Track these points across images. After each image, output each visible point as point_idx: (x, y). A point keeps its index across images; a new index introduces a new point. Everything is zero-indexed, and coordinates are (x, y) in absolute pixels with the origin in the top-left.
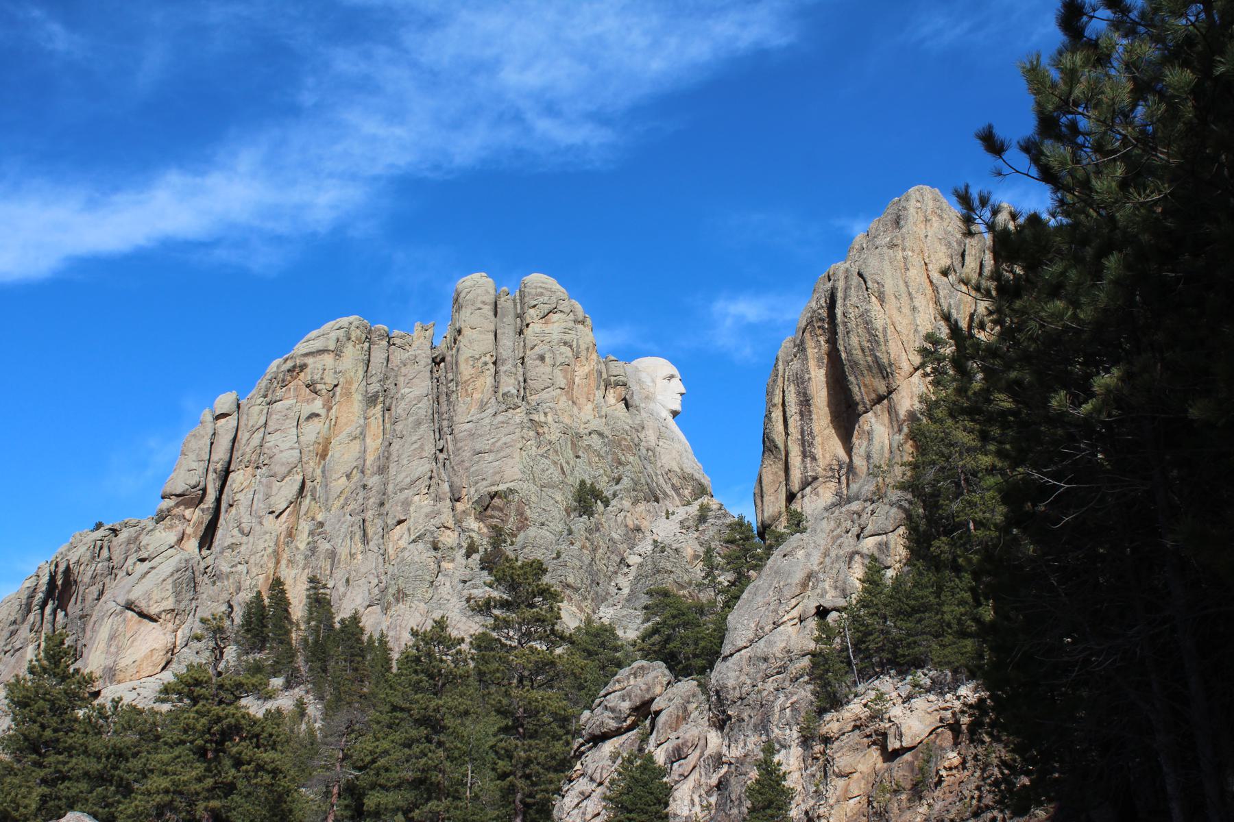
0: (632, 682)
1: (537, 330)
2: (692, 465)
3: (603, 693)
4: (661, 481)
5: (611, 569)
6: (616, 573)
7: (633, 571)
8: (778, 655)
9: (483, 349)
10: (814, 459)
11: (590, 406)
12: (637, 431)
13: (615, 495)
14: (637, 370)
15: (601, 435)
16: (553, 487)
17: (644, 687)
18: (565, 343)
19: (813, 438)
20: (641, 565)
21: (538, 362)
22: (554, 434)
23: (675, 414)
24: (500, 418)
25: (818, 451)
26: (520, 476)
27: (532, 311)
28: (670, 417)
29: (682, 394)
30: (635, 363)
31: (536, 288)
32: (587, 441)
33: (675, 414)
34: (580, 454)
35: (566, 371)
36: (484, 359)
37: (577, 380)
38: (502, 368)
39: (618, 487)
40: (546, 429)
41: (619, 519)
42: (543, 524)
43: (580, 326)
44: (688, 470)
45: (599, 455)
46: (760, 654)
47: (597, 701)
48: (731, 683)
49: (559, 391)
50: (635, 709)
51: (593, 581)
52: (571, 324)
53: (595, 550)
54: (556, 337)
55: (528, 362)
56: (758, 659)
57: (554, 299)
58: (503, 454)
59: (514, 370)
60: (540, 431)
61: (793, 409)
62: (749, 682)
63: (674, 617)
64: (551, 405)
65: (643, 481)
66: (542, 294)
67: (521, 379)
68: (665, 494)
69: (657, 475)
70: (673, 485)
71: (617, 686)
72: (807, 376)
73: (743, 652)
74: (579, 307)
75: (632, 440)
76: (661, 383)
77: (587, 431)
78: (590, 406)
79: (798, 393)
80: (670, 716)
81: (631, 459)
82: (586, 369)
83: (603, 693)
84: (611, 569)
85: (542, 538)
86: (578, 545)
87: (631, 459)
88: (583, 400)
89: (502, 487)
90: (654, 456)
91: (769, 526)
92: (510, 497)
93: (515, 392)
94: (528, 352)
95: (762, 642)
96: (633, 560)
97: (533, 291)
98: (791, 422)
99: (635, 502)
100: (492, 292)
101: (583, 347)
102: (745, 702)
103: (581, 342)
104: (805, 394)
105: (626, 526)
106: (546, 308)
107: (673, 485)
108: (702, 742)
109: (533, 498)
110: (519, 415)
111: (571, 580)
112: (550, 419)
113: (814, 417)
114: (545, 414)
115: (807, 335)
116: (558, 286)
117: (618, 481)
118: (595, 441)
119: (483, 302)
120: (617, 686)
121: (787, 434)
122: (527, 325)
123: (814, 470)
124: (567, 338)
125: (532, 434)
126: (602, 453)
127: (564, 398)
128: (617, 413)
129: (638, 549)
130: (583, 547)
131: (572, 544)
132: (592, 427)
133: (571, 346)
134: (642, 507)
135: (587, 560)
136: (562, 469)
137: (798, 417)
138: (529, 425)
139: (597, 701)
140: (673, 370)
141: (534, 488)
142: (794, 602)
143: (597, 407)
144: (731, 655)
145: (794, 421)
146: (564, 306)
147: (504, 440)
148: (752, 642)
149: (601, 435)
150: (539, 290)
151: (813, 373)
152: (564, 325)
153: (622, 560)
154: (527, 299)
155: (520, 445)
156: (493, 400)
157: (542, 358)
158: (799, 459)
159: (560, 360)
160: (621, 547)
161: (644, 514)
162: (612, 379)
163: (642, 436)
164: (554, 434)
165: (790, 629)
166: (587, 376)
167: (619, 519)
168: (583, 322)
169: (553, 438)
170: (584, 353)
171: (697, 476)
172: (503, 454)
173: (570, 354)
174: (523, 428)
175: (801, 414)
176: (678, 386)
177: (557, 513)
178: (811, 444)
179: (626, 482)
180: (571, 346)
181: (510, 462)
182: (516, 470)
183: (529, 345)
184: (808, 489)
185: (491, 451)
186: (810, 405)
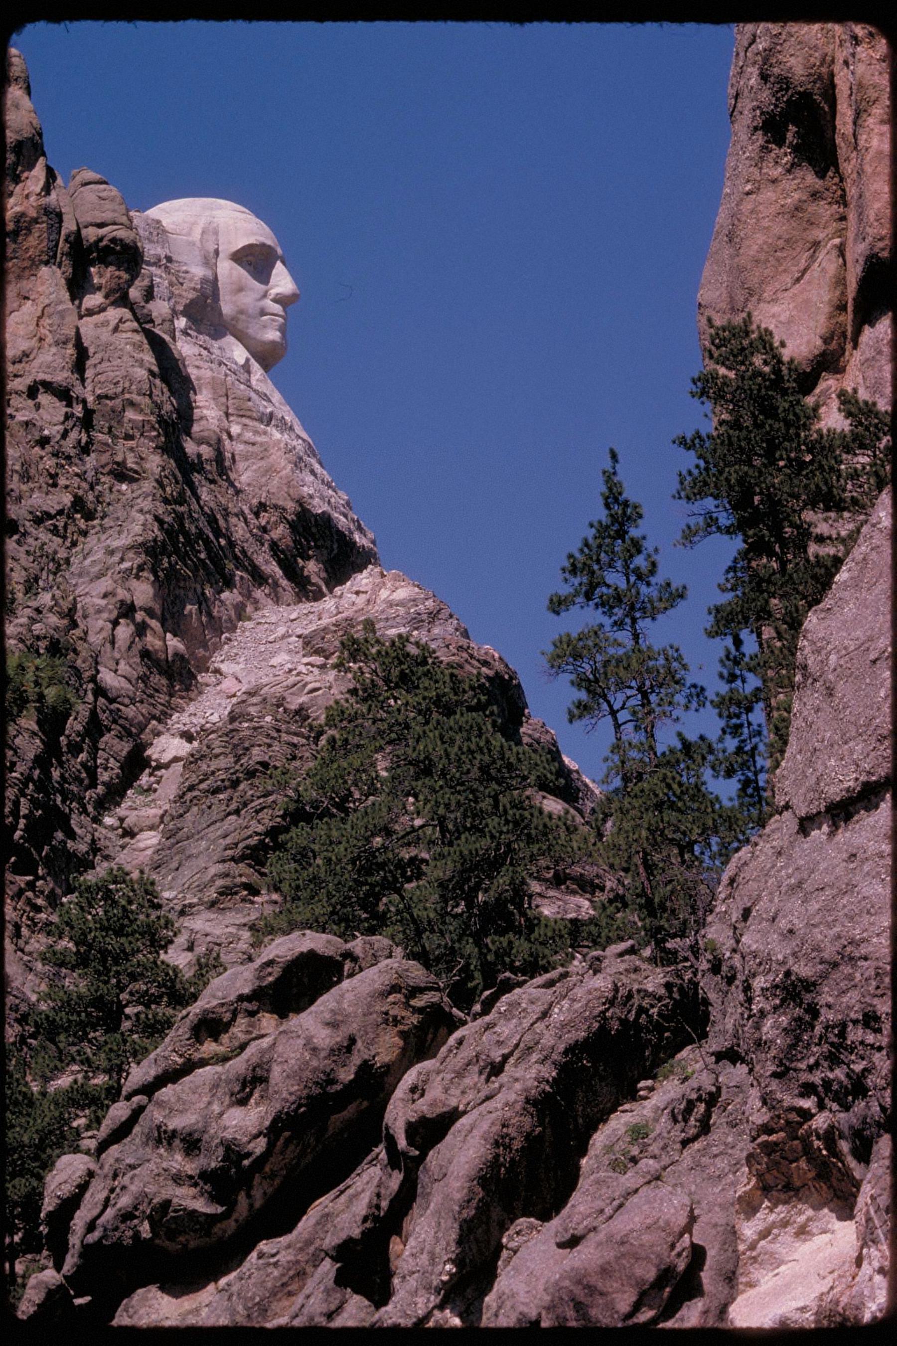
2: (322, 495)
3: (139, 1073)
4: (239, 531)
7: (170, 784)
15: (64, 394)
20: (193, 760)
33: (267, 356)
44: (318, 507)
45: (56, 455)
69: (226, 514)
80: (500, 1142)
83: (139, 1073)
91: (618, 594)
105: (145, 654)
132: (35, 372)
160: (130, 712)
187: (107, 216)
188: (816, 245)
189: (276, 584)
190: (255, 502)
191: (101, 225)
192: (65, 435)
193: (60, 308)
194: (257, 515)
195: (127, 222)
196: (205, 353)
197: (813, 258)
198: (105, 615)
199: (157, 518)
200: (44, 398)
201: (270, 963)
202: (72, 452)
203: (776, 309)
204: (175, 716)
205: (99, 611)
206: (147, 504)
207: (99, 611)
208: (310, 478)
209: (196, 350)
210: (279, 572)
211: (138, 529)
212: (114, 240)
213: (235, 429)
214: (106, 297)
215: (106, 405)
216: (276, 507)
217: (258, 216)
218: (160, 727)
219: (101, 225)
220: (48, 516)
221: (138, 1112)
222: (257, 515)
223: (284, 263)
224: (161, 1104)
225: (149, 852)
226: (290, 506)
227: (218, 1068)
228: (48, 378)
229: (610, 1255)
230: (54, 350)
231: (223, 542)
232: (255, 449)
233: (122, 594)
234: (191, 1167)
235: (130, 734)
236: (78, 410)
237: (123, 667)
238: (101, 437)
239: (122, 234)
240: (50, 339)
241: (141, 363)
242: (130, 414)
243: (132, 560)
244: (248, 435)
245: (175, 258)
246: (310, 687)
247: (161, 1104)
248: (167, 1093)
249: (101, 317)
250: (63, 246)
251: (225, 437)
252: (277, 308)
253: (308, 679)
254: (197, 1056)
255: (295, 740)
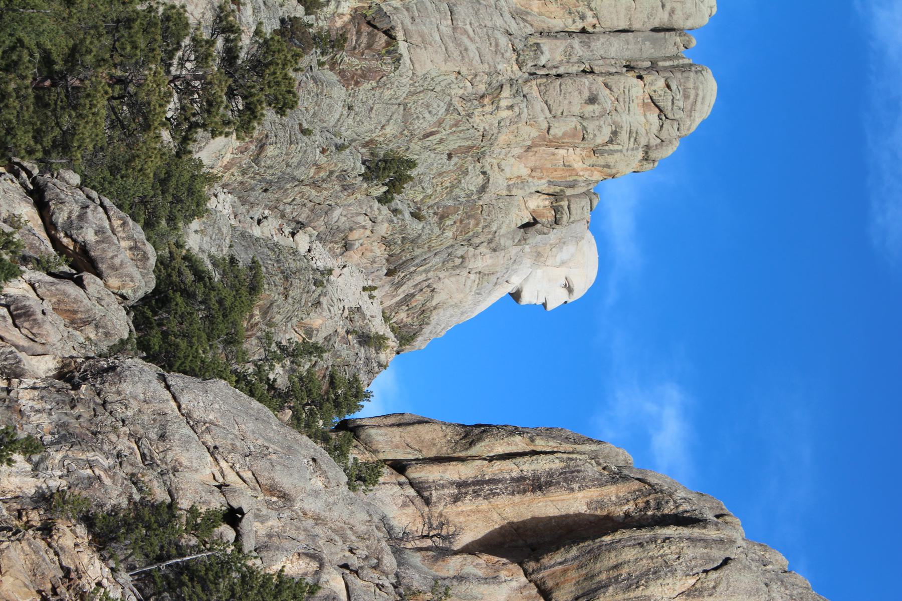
0: (124, 244)
1: (634, 92)
2: (442, 322)
3: (107, 202)
4: (419, 278)
5: (288, 209)
6: (283, 216)
7: (286, 241)
8: (170, 454)
9: (604, 13)
10: (456, 499)
11: (524, 172)
12: (490, 241)
13: (395, 211)
14: (579, 239)
15: (483, 189)
16: (405, 121)
17: (117, 261)
18: (615, 133)
19: (486, 498)
20: (295, 252)
21: (586, 94)
22: (482, 120)
23: (516, 296)
24: (503, 41)
25: (467, 505)
26: (420, 72)
27: (661, 83)
28: (511, 288)
29: (545, 305)
30: (589, 235)
31: (696, 88)
32: (474, 169)
33: (516, 296)
34: (455, 160)
35: (574, 136)
36: (589, 14)
37: (562, 152)
38: (576, 42)
39: (407, 215)
40: (488, 109)
41: (361, 219)
42: (350, 108)
43: (640, 154)
44: (434, 318)
45: (452, 186)
46: (171, 428)
47: (94, 194)
48: (127, 387)
49: (545, 126)
50: (84, 250)
51: (270, 183)
52: (643, 141)
53: (315, 184)
54: (624, 119)
55: (586, 80)
56: (163, 427)
57: (679, 115)
58: (451, 46)
59: (574, 59)
60: (486, 101)
61: (528, 467)
62: (130, 413)
63: (221, 302)
64: (525, 116)
65: (418, 252)
66: (686, 97)
67: (561, 71)
68: (399, 285)
70: (413, 295)
71: (117, 223)
72: (575, 486)
73: (173, 404)
74: (669, 151)
75: (476, 235)
76: (560, 274)
77: (487, 168)
78: (524, 172)
79: (550, 474)
80: (76, 301)
81: (449, 234)
82: (578, 165)
83: (107, 202)
84: (288, 209)
85: (330, 107)
86: (322, 160)
87: (449, 234)
88: (532, 161)
89: (402, 47)
90: (455, 267)
91: (357, 437)
92: (388, 59)
93: (543, 61)
94: (600, 79)
95: (187, 431)
96: (303, 241)
97: (690, 85)
98: (508, 464)
99: (385, 241)
100: (689, 24)
101: (611, 160)
102: (100, 410)
103: (617, 156)
104: (549, 484)
105: (351, 229)
106: (666, 104)
107: (413, 295)
108: (39, 349)
109: (388, 93)
110: (508, 68)
111: (270, 150)
112: (504, 114)
113: (517, 498)
114: (511, 107)
115: (636, 485)
116: (698, 121)
117: (416, 216)
118: (473, 181)
119: (672, 12)
120: (117, 223)
121: (491, 459)
122: (640, 77)
123: (439, 499)
124: (623, 136)
125: (482, 88)
126: (457, 191)
127: (535, 133)
128: (514, 212)
129: (317, 245)
130: (319, 168)
131: (323, 151)
133: (611, 141)
134: (380, 251)
135: (300, 173)
136: (432, 134)
137: (515, 474)
138: (495, 84)
139: (94, 194)
140: (580, 291)
141: (402, 93)
142: (248, 475)
143: (522, 182)
144: (168, 387)
145: (510, 469)
146: (670, 130)
147: (472, 47)
148: (188, 416)
149: (483, 189)
150: (692, 93)
151: (580, 495)
152: (642, 131)
153: (300, 226)
154: (679, 75)
155: (464, 71)
156: (530, 30)
157: (592, 100)
158: (456, 478)
159: (591, 126)
160: (321, 222)
161: (369, 254)
162: (565, 203)
163: (483, 249)
164: (482, 120)
165: (208, 471)
166: (568, 167)
167: (361, 219)
168: (646, 158)
169: (476, 120)
170: (601, 161)
171: (427, 330)
172: (451, 46)
173: (600, 140)
174: (489, 74)
175: (521, 479)
176: (556, 299)
177: (368, 129)
178: (476, 494)
179: (415, 227)
180: (611, 141)
181: (440, 58)
182: (429, 66)
183: (611, 80)
184: (411, 492)
185: (455, 29)
186: (533, 491)
187: (573, 211)
188: (421, 451)
189: (394, 296)
190: (434, 286)
191: (569, 208)
192: (463, 190)
193: (526, 188)
194: (428, 286)
195: (571, 220)
196: (512, 261)
197: (415, 450)
198: (369, 210)
199: (420, 235)
200: (480, 179)
201: (144, 244)
202: (454, 194)
203: (398, 437)
204: (320, 245)
205: (371, 207)
206: (427, 231)
207: (371, 207)
208: (448, 314)
209: (514, 258)
210: (398, 298)
211: (414, 226)
212: (562, 213)
213: (472, 276)
214: (534, 211)
215: (478, 209)
216: (433, 297)
217: (589, 290)
218: (314, 238)
219: (569, 208)
220: (421, 182)
221: (93, 201)
222: (428, 286)
223: (566, 302)
224: (96, 207)
225: (250, 231)
226: (434, 303)
227: (108, 227)
228: (491, 181)
229: (40, 321)
230: (505, 184)
231: (412, 269)
232: (462, 286)
233: (380, 218)
234: (74, 216)
235: (310, 222)
236: (475, 197)
237: (343, 219)
238: (462, 208)
239: (565, 218)
240: (511, 183)
241: (499, 228)
242: (472, 222)
243: (398, 223)
244: (469, 283)
245: (565, 248)
246: (331, 308)
247: (96, 207)
248: (100, 209)
249: (523, 207)
250: (558, 189)
251: (468, 270)
252: (542, 301)
253: (336, 307)
254: (113, 219)
255: (303, 300)
